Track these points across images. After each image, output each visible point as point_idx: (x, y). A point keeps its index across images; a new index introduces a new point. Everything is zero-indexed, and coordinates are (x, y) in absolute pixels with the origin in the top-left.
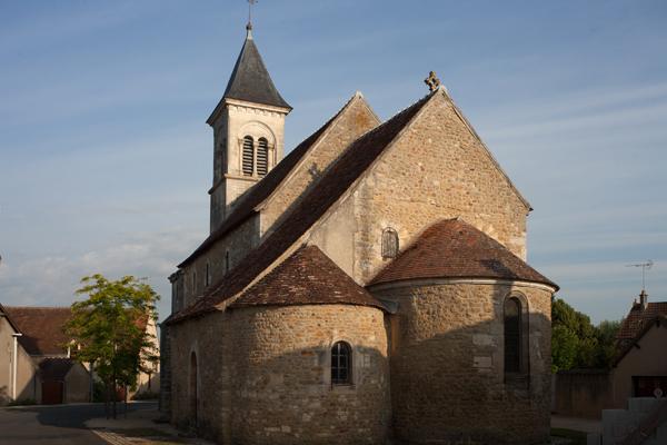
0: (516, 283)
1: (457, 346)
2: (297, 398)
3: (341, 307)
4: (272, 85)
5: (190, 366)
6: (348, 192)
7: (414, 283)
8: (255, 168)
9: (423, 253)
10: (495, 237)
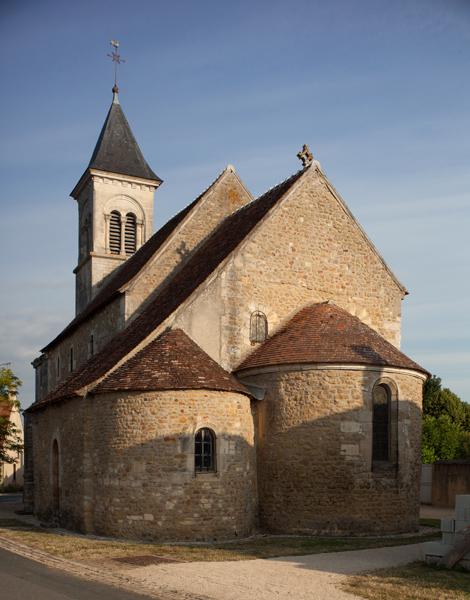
0: (386, 369)
1: (324, 433)
2: (160, 486)
3: (205, 392)
4: (141, 157)
5: (51, 455)
6: (216, 272)
7: (281, 368)
8: (123, 246)
10: (368, 322)
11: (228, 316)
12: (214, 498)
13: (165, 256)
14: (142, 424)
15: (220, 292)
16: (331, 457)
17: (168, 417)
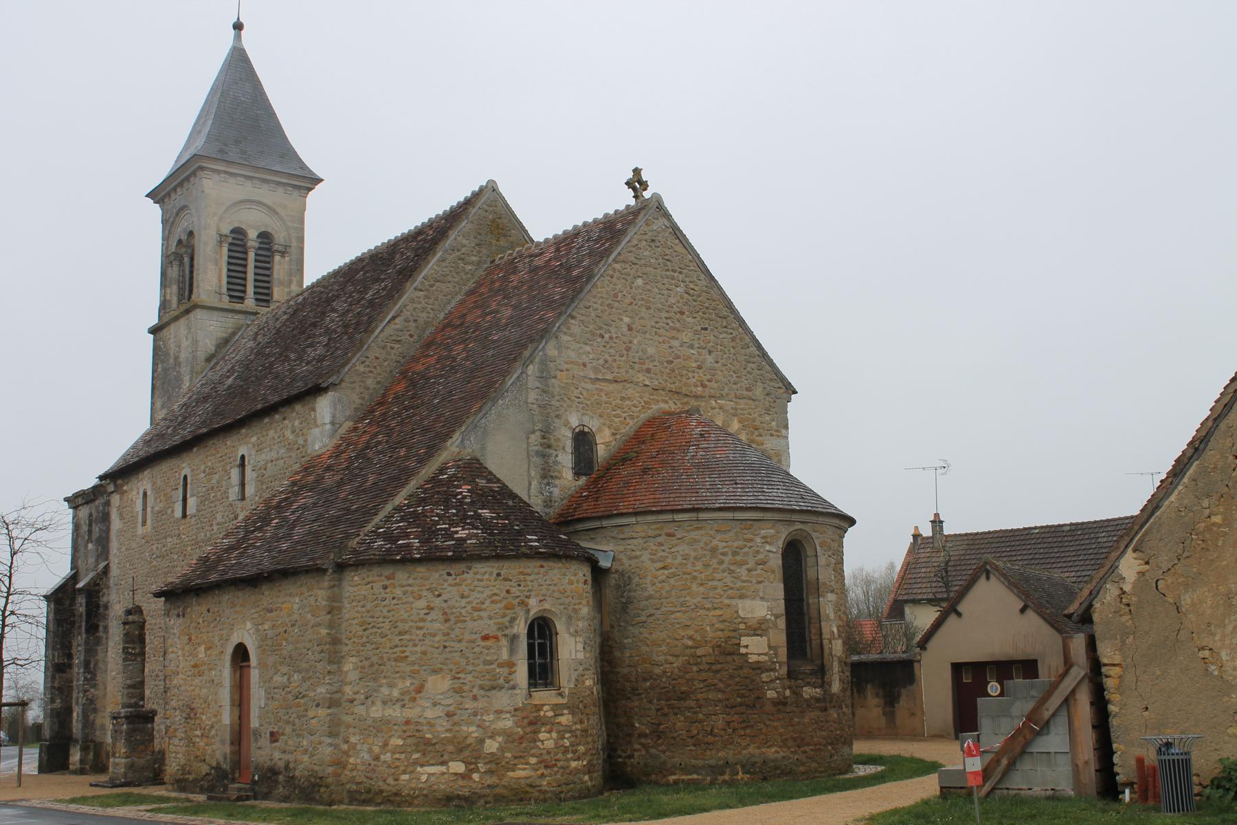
1: (715, 620)
2: (475, 714)
8: (250, 289)
9: (645, 471)
11: (538, 433)
12: (559, 732)
13: (392, 326)
15: (527, 397)
17: (487, 603)
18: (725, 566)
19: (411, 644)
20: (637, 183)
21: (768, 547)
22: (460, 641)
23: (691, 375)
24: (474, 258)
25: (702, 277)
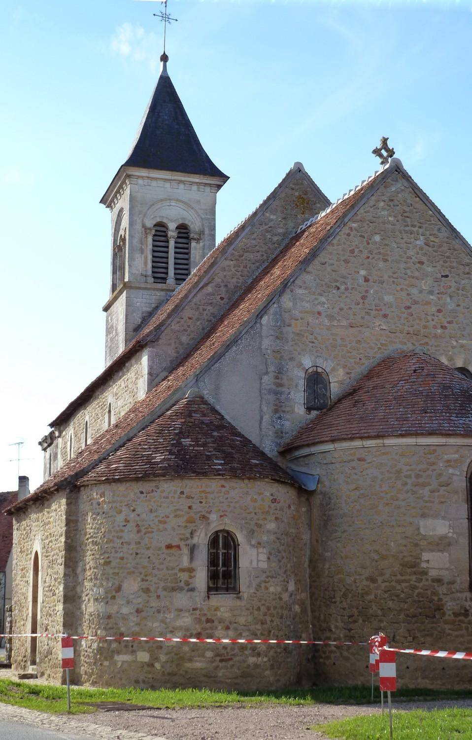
2: (159, 611)
8: (171, 272)
11: (271, 375)
12: (236, 629)
14: (138, 525)
15: (260, 343)
16: (409, 570)
18: (409, 487)
19: (113, 550)
20: (384, 150)
21: (451, 471)
22: (148, 548)
23: (430, 318)
24: (280, 231)
25: (444, 229)
